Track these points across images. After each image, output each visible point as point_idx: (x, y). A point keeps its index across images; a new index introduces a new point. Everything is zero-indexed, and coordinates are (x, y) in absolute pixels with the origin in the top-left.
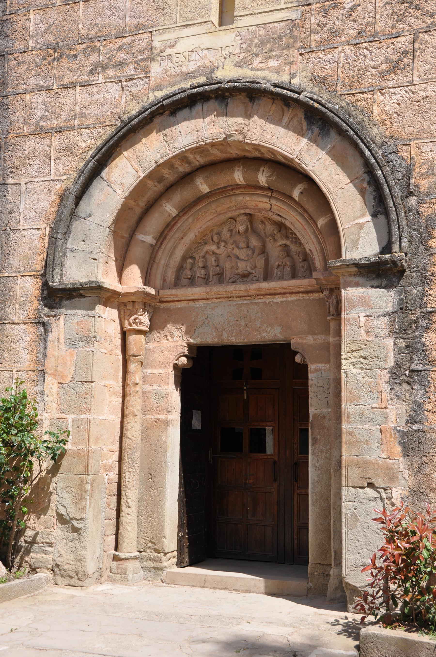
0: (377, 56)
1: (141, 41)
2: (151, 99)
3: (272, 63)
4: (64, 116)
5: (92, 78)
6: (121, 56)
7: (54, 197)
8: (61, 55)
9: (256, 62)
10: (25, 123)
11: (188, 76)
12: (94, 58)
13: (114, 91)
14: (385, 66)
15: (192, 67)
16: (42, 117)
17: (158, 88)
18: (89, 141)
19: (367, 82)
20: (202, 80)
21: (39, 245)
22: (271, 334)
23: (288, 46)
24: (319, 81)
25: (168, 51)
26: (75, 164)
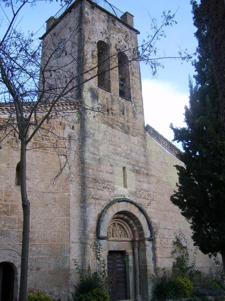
0: (146, 202)
1: (112, 184)
2: (115, 198)
3: (133, 198)
4: (98, 196)
5: (103, 189)
6: (109, 187)
7: (97, 215)
8: (97, 182)
9: (131, 196)
10: (90, 195)
11: (121, 196)
12: (103, 185)
13: (107, 193)
14: (147, 204)
15: (121, 194)
16: (93, 195)
17: (116, 196)
18: (104, 203)
19: (146, 206)
20: (123, 197)
21: (94, 226)
22: (123, 249)
23: (135, 196)
24: (140, 204)
25: (117, 189)
26: (101, 208)
